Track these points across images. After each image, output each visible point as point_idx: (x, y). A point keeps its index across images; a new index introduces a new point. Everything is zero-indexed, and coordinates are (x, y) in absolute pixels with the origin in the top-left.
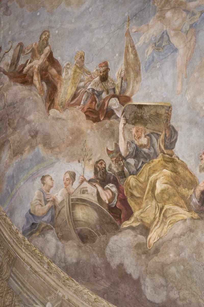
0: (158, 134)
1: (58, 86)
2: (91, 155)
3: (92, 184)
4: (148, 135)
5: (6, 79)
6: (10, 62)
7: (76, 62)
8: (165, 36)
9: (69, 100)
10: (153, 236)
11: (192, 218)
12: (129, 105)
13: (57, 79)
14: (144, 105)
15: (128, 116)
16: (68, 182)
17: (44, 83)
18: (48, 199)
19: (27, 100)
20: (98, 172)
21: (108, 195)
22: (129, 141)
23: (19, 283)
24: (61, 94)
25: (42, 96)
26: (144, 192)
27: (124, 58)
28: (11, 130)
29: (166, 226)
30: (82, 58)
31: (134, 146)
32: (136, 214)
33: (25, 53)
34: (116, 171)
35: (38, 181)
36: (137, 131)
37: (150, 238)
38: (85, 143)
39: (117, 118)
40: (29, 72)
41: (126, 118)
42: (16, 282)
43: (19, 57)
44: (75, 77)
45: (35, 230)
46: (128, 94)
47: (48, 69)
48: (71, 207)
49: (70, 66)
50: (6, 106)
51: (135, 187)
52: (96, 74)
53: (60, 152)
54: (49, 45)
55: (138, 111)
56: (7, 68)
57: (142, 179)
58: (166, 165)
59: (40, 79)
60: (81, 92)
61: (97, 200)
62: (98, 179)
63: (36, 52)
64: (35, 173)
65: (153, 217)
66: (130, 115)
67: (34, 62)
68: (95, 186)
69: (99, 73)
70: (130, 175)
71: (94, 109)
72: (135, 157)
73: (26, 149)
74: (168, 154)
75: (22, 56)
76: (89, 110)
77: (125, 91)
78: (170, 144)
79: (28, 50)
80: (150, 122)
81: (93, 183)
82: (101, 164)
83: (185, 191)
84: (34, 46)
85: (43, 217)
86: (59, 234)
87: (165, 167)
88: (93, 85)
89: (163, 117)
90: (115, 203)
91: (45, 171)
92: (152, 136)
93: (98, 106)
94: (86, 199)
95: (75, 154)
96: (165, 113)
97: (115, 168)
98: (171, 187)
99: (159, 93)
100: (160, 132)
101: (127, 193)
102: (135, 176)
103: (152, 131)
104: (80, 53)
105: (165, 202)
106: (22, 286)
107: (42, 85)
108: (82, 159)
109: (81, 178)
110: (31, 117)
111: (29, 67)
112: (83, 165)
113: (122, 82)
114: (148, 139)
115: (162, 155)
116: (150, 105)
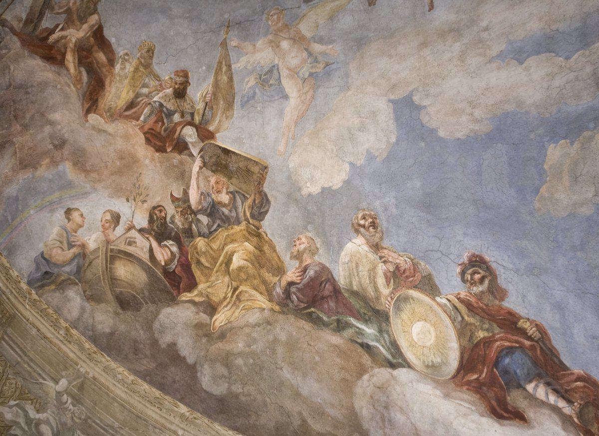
0: (244, 196)
1: (107, 82)
2: (147, 195)
4: (231, 193)
5: (16, 44)
6: (24, 16)
8: (275, 72)
9: (121, 108)
10: (220, 319)
11: (272, 310)
12: (211, 144)
13: (106, 71)
14: (232, 151)
15: (207, 158)
16: (108, 225)
17: (83, 69)
18: (74, 242)
19: (50, 87)
20: (154, 221)
21: (165, 254)
22: (204, 191)
23: (17, 350)
24: (111, 96)
25: (78, 89)
26: (216, 263)
27: (214, 76)
28: (19, 127)
29: (239, 311)
30: (151, 52)
31: (210, 200)
32: (201, 287)
33: (55, 12)
34: (181, 227)
35: (60, 214)
36: (217, 183)
37: (216, 320)
38: (140, 176)
39: (191, 155)
40: (60, 44)
41: (204, 159)
42: (12, 348)
43: (41, 15)
44: (135, 77)
45: (48, 281)
46: (211, 128)
47: (93, 50)
49: (129, 58)
50: (12, 86)
51: (204, 253)
53: (100, 181)
54: (98, 14)
55: (222, 156)
56: (18, 24)
57: (215, 246)
58: (250, 237)
60: (143, 102)
61: (148, 258)
62: (153, 230)
63: (75, 17)
65: (224, 295)
66: (211, 157)
67: (69, 31)
68: (147, 238)
69: (173, 84)
70: (200, 236)
71: (160, 133)
72: (209, 215)
73: (42, 163)
74: (254, 226)
75: (48, 14)
76: (152, 131)
79: (60, 8)
80: (236, 176)
81: (145, 234)
82: (161, 211)
83: (268, 276)
84: (71, 4)
85: (64, 266)
86: (87, 293)
87: (247, 240)
88: (162, 98)
89: (255, 177)
90: (174, 267)
91: (73, 201)
92: (237, 195)
93: (165, 130)
94: (133, 253)
95: (122, 189)
96: (259, 172)
97: (179, 221)
99: (254, 143)
100: (248, 194)
101: (192, 258)
102: (206, 239)
103: (237, 189)
104: (148, 44)
105: (241, 282)
106: (22, 355)
107: (80, 72)
108: (132, 198)
109: (129, 224)
110: (56, 116)
111: (60, 36)
112: (133, 207)
113: (205, 108)
114: (230, 198)
115: (246, 224)
116: (240, 155)
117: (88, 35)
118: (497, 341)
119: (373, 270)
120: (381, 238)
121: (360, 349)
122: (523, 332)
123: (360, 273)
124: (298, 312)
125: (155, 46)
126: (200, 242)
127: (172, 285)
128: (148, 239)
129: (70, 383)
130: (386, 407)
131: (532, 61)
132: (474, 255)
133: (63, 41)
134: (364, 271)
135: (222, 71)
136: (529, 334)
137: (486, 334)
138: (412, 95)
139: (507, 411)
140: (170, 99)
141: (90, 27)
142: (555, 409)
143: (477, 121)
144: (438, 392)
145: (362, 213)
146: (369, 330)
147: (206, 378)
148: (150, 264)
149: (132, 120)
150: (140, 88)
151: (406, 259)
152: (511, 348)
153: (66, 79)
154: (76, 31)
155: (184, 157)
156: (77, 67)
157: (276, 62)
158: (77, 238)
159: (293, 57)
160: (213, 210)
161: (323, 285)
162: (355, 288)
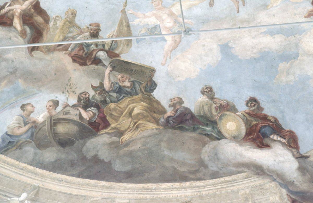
0: (140, 82)
1: (44, 33)
3: (75, 108)
4: (132, 81)
7: (66, 16)
8: (158, 28)
10: (126, 137)
12: (117, 59)
16: (51, 108)
18: (28, 121)
20: (82, 100)
22: (113, 82)
24: (47, 39)
26: (122, 113)
27: (118, 27)
29: (138, 132)
31: (118, 85)
32: (113, 125)
36: (122, 77)
39: (104, 65)
44: (64, 28)
45: (11, 146)
46: (117, 52)
48: (52, 125)
52: (86, 30)
58: (144, 100)
59: (22, 23)
61: (78, 118)
62: (81, 104)
64: (14, 102)
67: (14, 6)
70: (111, 102)
71: (82, 56)
72: (117, 93)
74: (147, 95)
76: (76, 55)
77: (114, 49)
78: (150, 90)
80: (134, 74)
82: (85, 95)
87: (143, 101)
92: (135, 82)
93: (86, 54)
94: (68, 118)
98: (145, 112)
101: (106, 114)
103: (135, 80)
105: (139, 120)
108: (66, 91)
109: (65, 104)
112: (67, 96)
114: (131, 83)
116: (137, 64)
117: (29, 8)
118: (260, 124)
119: (210, 108)
120: (214, 95)
121: (204, 136)
122: (269, 120)
123: (205, 109)
124: (173, 128)
125: (76, 11)
126: (112, 105)
127: (94, 128)
128: (78, 109)
129: (28, 194)
130: (216, 154)
131: (276, 36)
132: (251, 98)
133: (11, 12)
134: (206, 108)
135: (123, 25)
136: (271, 121)
137: (256, 123)
138: (228, 43)
139: (263, 145)
140: (88, 38)
141: (30, 3)
142: (280, 142)
143: (254, 53)
144: (237, 145)
145: (205, 87)
146: (208, 129)
147: (118, 165)
148: (79, 121)
149: (63, 51)
150: (68, 34)
151: (224, 101)
152: (265, 125)
153: (15, 34)
154: (20, 6)
155: (99, 67)
156: (22, 26)
157: (158, 23)
158: (30, 119)
159: (168, 23)
160: (120, 90)
161: (186, 115)
162: (202, 114)
